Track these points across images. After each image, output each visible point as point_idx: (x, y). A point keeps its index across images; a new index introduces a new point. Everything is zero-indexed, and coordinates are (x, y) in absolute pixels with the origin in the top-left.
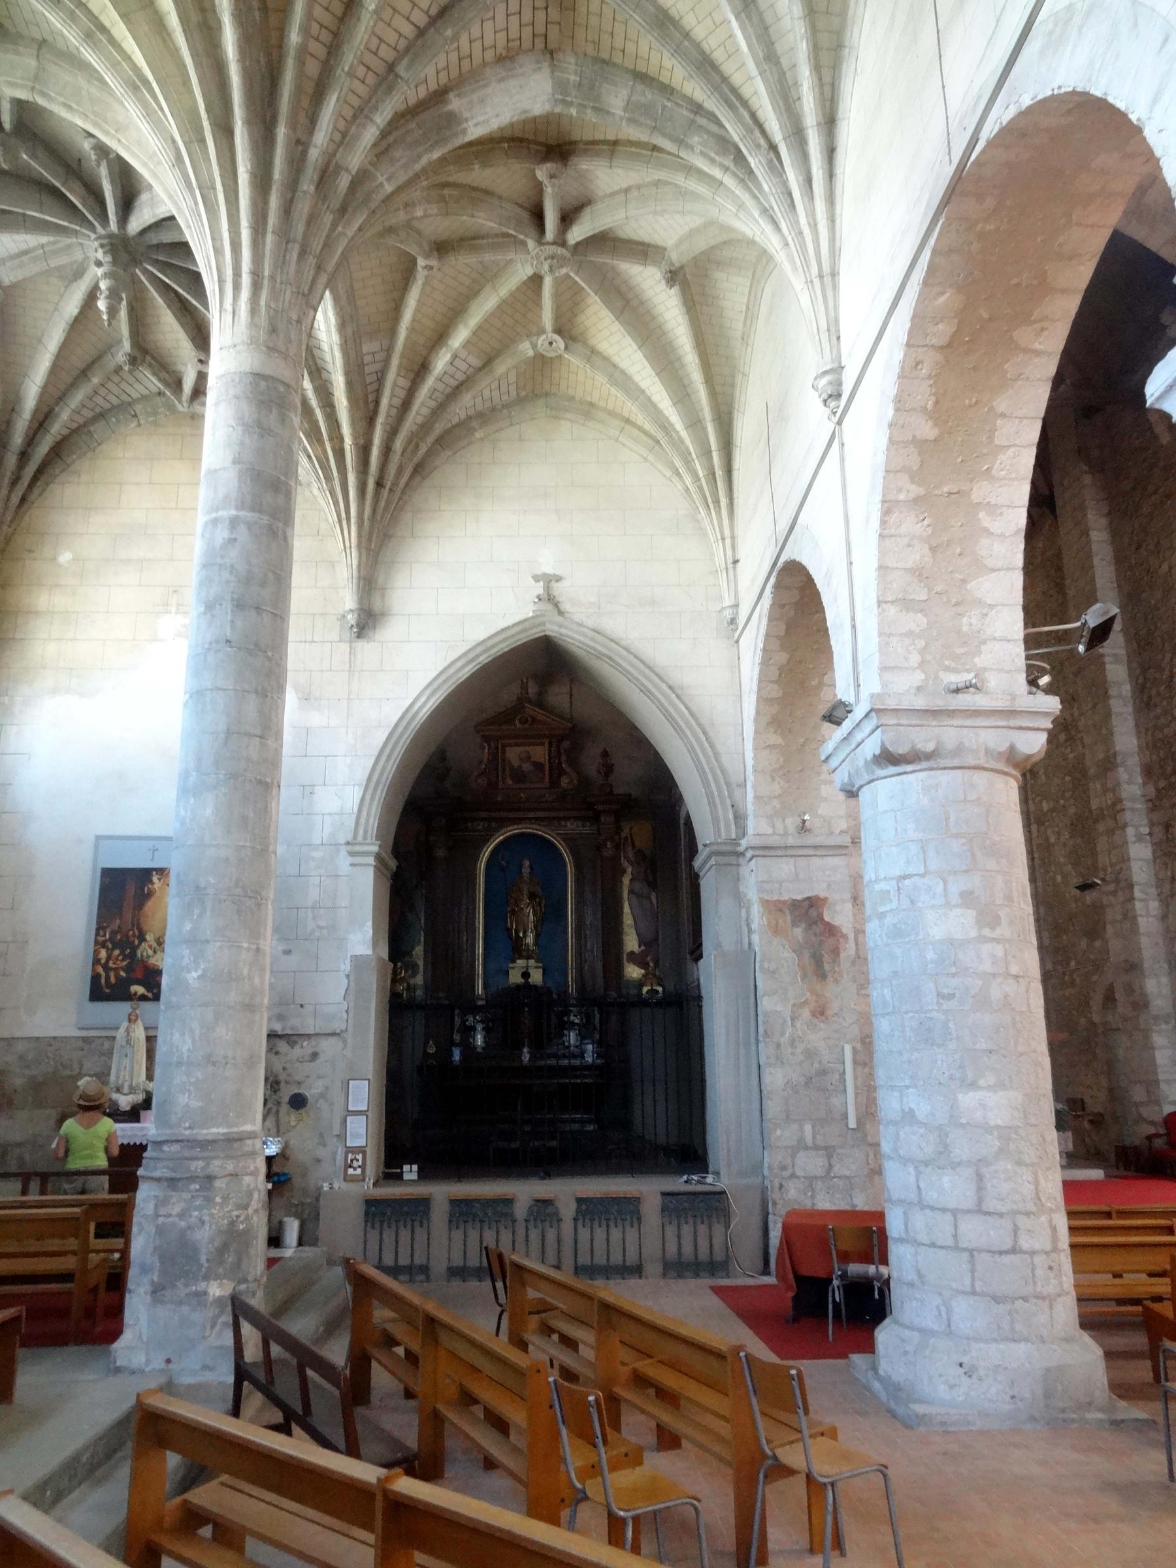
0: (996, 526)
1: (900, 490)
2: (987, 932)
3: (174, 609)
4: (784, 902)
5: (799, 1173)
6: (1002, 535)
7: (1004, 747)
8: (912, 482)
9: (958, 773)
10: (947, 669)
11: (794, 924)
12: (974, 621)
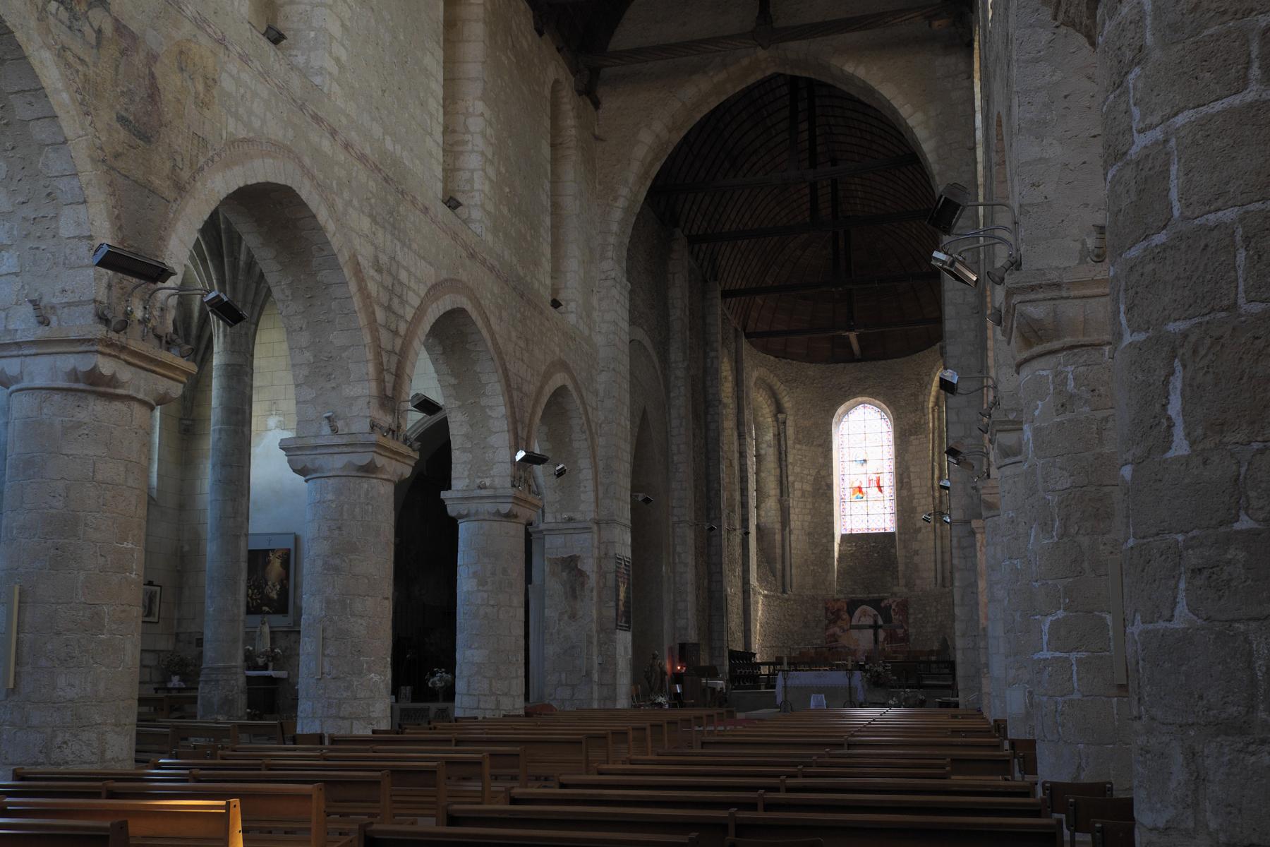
1: (452, 404)
2: (481, 588)
3: (274, 413)
4: (557, 559)
6: (497, 418)
7: (495, 510)
8: (456, 400)
10: (479, 477)
11: (562, 571)
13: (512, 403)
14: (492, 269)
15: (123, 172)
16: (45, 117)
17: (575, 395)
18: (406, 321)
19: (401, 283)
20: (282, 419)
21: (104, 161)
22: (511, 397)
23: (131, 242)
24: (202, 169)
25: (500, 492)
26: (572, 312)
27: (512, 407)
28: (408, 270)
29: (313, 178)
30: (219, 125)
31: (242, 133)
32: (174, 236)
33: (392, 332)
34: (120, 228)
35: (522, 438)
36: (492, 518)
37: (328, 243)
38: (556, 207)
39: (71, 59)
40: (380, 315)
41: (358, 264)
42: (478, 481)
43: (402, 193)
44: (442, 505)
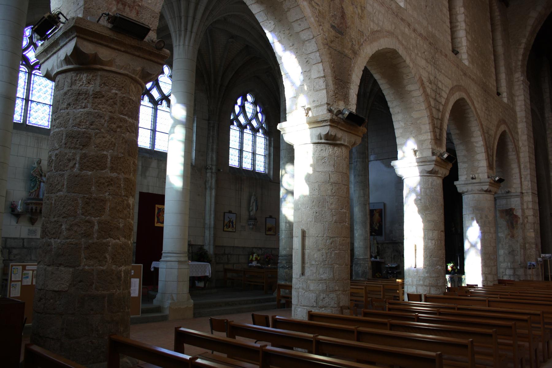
0: (478, 145)
5: (507, 274)
7: (480, 189)
9: (472, 195)
10: (471, 174)
12: (477, 164)
13: (485, 139)
14: (473, 80)
15: (334, 48)
16: (305, 29)
17: (509, 135)
18: (442, 105)
19: (439, 88)
20: (376, 156)
21: (327, 44)
22: (485, 136)
23: (339, 78)
24: (362, 44)
25: (482, 181)
26: (505, 97)
27: (486, 142)
28: (441, 82)
29: (403, 45)
30: (367, 26)
31: (376, 28)
32: (354, 73)
33: (437, 110)
34: (334, 72)
35: (491, 155)
36: (479, 192)
37: (411, 72)
38: (495, 51)
39: (314, 4)
40: (432, 103)
41: (422, 81)
42: (471, 176)
43: (437, 49)
44: (455, 188)
